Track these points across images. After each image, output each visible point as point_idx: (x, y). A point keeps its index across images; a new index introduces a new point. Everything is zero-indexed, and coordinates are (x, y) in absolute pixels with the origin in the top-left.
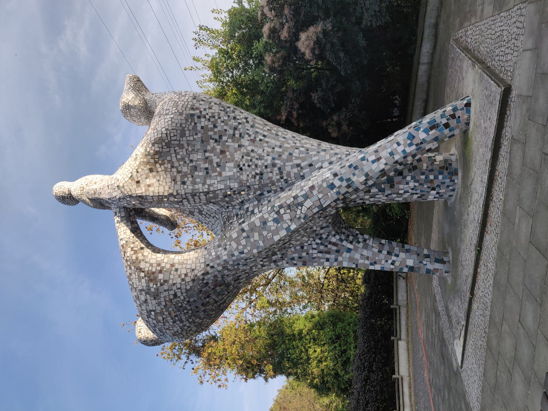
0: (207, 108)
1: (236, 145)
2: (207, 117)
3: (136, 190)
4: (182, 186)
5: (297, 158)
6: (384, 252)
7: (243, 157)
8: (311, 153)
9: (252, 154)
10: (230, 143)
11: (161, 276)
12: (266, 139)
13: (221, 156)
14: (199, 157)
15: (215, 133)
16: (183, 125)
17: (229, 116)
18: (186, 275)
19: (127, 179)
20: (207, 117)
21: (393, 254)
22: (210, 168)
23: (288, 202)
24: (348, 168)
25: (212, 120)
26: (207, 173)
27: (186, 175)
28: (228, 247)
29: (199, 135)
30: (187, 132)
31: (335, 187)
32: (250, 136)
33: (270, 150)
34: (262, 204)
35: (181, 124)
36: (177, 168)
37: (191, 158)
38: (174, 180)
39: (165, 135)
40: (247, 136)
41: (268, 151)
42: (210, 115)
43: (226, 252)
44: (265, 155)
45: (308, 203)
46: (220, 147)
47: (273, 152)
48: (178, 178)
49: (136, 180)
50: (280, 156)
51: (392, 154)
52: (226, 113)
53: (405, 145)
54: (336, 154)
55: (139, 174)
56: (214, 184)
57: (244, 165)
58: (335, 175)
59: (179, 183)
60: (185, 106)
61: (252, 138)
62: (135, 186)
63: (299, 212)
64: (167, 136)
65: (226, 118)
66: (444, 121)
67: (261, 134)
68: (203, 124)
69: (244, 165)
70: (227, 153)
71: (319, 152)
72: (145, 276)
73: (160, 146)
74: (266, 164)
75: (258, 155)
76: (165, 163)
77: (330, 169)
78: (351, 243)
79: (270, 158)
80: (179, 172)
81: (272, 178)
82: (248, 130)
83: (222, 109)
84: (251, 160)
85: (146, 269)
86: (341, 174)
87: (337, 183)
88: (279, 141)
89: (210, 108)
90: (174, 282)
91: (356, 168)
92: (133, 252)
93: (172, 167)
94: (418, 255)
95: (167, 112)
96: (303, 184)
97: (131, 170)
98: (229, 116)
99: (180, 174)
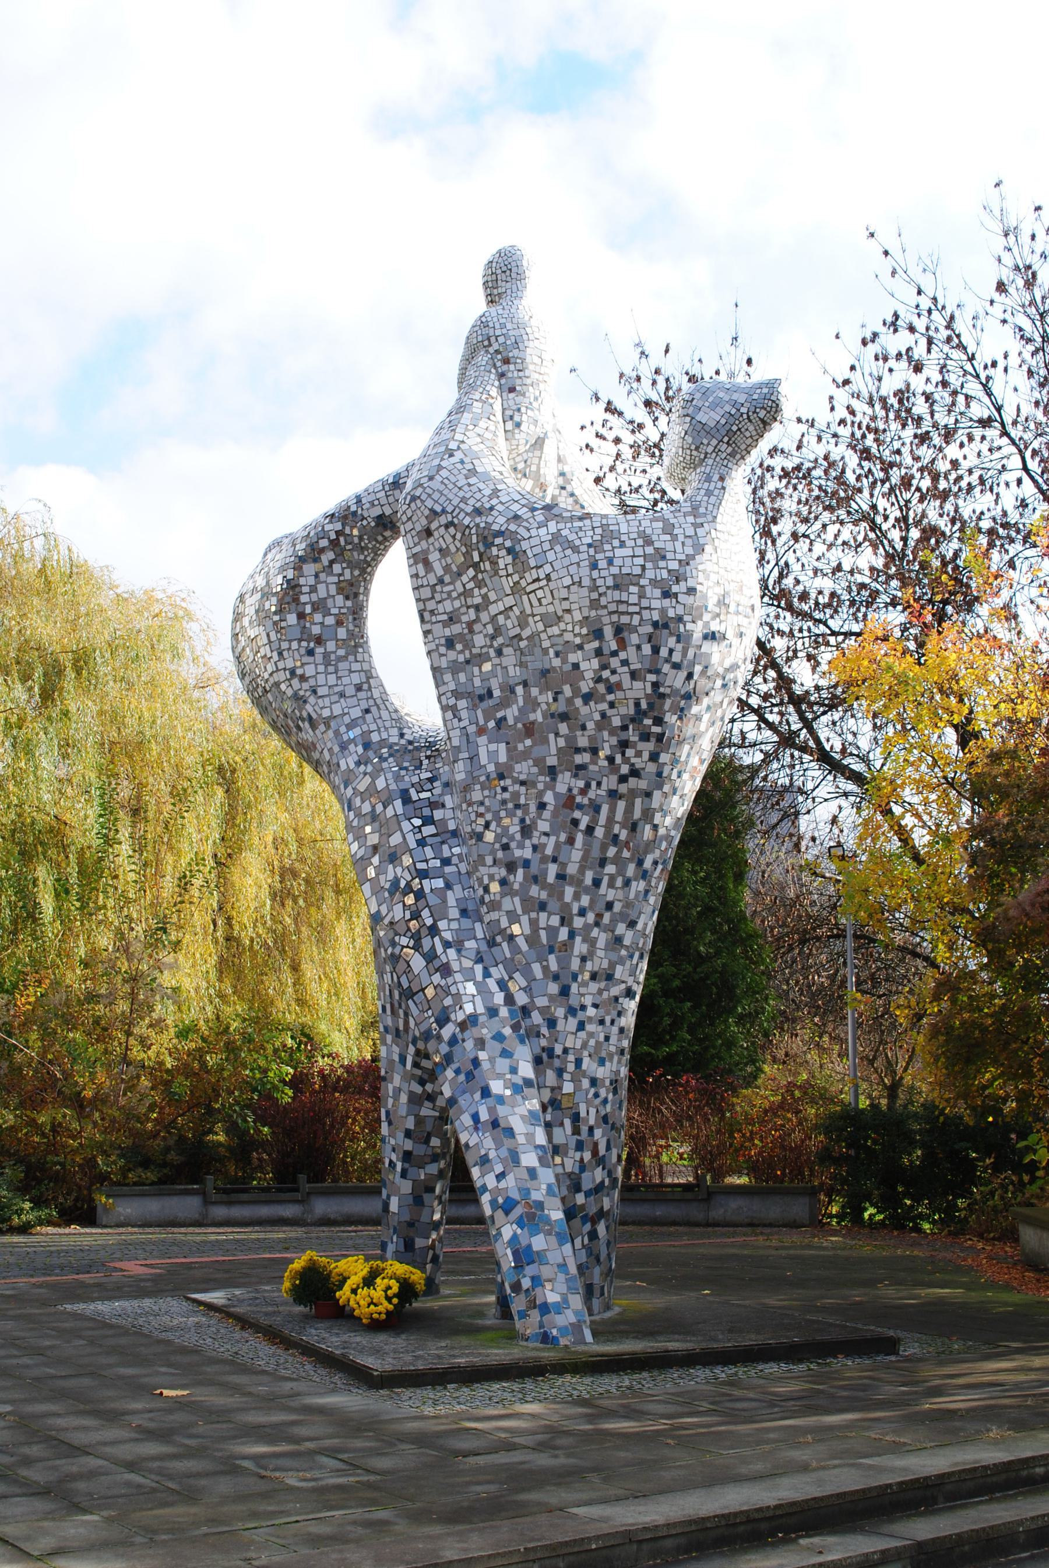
0: (632, 667)
1: (552, 761)
2: (606, 674)
3: (414, 533)
4: (443, 641)
5: (534, 923)
6: (408, 1145)
7: (523, 783)
8: (552, 958)
9: (533, 808)
10: (555, 744)
11: (292, 619)
12: (580, 838)
13: (520, 725)
14: (511, 673)
15: (570, 701)
16: (567, 617)
17: (624, 728)
18: (303, 678)
19: (429, 503)
20: (606, 674)
21: (407, 1165)
22: (491, 702)
23: (425, 913)
24: (472, 1056)
25: (601, 688)
26: (481, 698)
27: (468, 645)
28: (362, 768)
29: (557, 662)
30: (555, 630)
31: (441, 1028)
32: (583, 792)
33: (549, 851)
34: (443, 842)
35: (568, 611)
36: (477, 620)
37: (506, 651)
38: (451, 619)
39: (535, 576)
40: (581, 784)
41: (545, 845)
42: (614, 679)
43: (352, 766)
44: (535, 841)
45: (418, 963)
46: (540, 719)
47: (544, 860)
48: (456, 629)
49: (433, 526)
50: (535, 879)
51: (484, 1160)
52: (633, 720)
53: (497, 1191)
54: (552, 1023)
55: (442, 530)
56: (460, 720)
57: (504, 789)
58: (463, 1026)
59: (447, 632)
60: (622, 608)
61: (578, 799)
62: (418, 528)
63: (404, 941)
64: (534, 581)
65: (616, 722)
66: (526, 1283)
67: (594, 821)
68: (584, 666)
69: (504, 789)
70: (528, 742)
71: (556, 977)
72: (288, 581)
73: (510, 571)
74: (513, 845)
75: (534, 823)
76: (480, 588)
77: (493, 1012)
78: (416, 1065)
79: (527, 853)
80: (470, 625)
81: (484, 865)
82: (599, 784)
83: (644, 705)
84: (517, 806)
85: (302, 581)
86: (463, 1041)
87: (447, 1032)
88: (582, 870)
89: (634, 675)
90: (285, 653)
91: (470, 1076)
92: (333, 536)
93: (477, 608)
94: (411, 1224)
95: (603, 564)
96: (470, 944)
97: (449, 509)
98: (624, 728)
99: (466, 631)
